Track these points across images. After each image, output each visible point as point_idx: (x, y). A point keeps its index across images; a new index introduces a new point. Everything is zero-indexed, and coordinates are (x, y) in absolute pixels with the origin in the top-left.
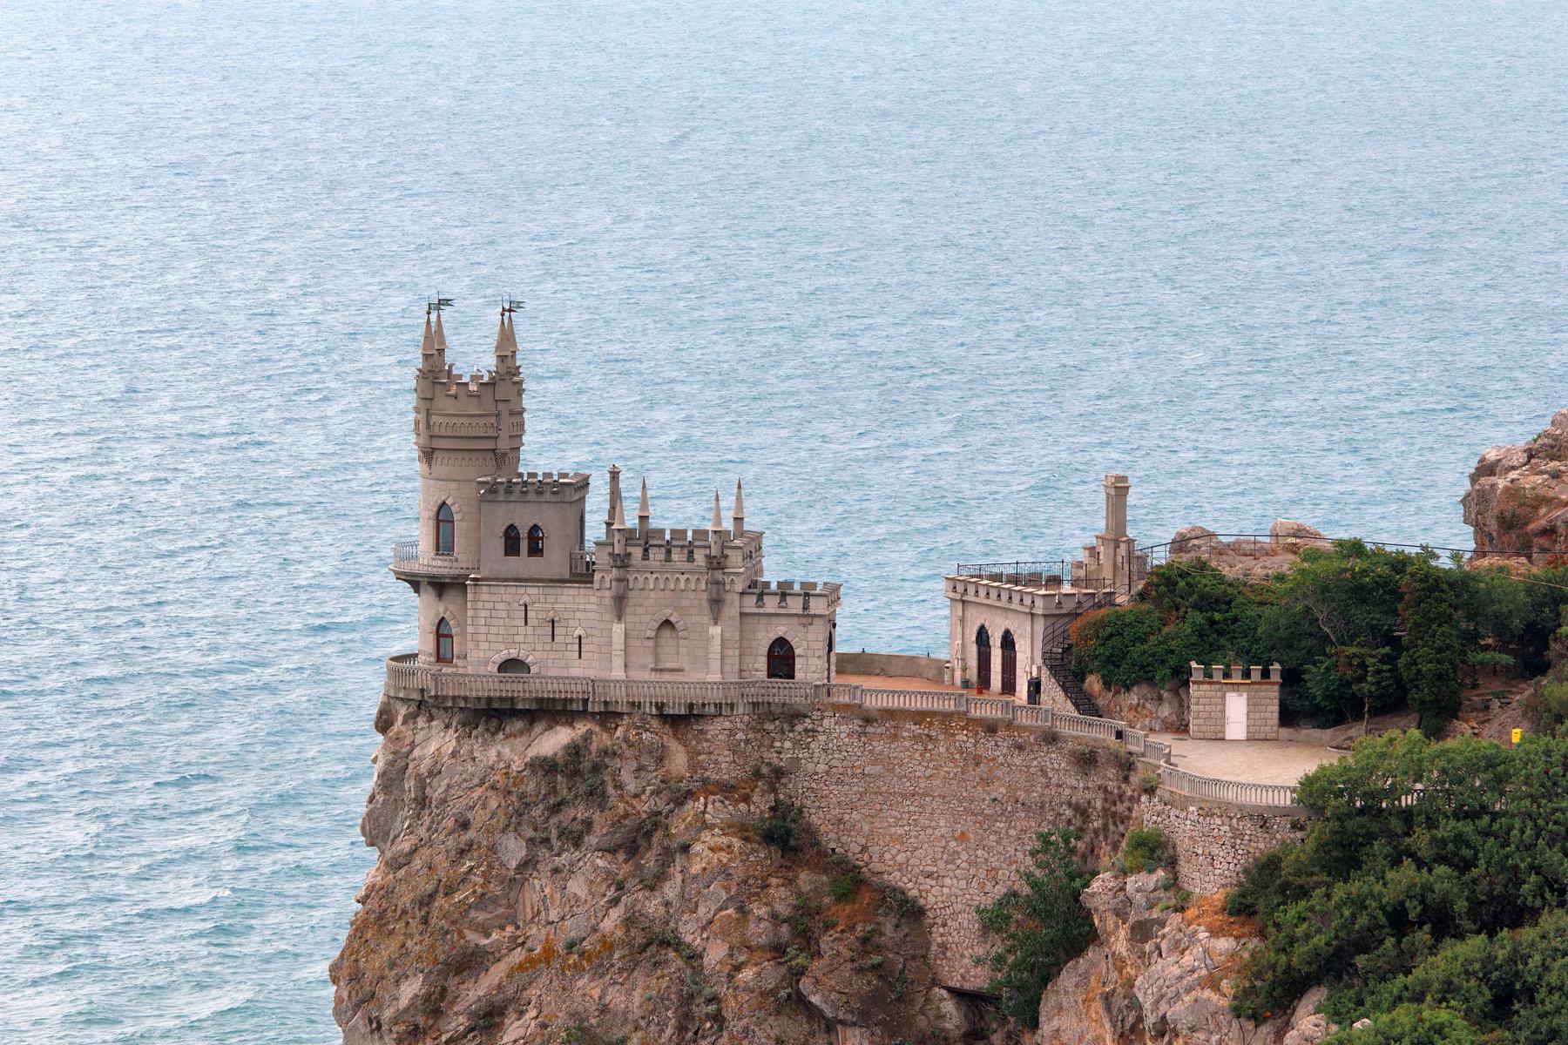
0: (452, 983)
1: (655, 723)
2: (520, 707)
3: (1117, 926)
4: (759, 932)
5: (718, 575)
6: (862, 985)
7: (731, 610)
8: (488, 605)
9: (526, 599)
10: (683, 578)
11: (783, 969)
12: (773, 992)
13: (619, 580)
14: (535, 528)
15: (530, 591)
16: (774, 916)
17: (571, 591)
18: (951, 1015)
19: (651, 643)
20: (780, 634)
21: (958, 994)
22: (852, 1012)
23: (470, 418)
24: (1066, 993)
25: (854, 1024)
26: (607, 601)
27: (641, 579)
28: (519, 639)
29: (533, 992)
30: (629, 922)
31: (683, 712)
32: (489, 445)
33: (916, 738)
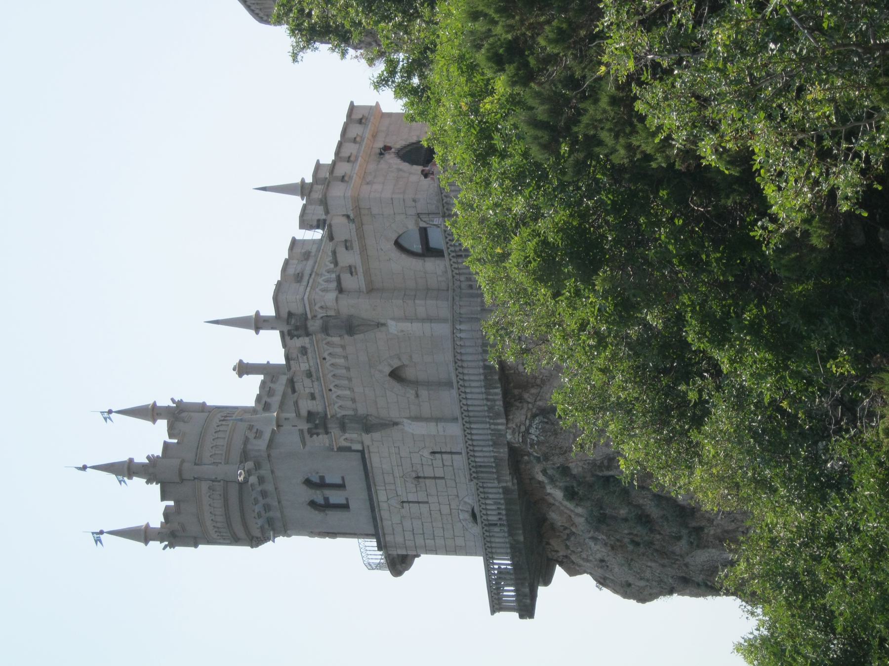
1: (520, 416)
2: (521, 538)
5: (314, 325)
7: (362, 307)
8: (409, 535)
9: (393, 502)
10: (330, 360)
13: (343, 427)
14: (308, 482)
15: (382, 496)
17: (375, 461)
19: (424, 393)
20: (390, 245)
23: (220, 484)
26: (376, 435)
27: (340, 403)
28: (445, 510)
31: (498, 391)
32: (233, 492)
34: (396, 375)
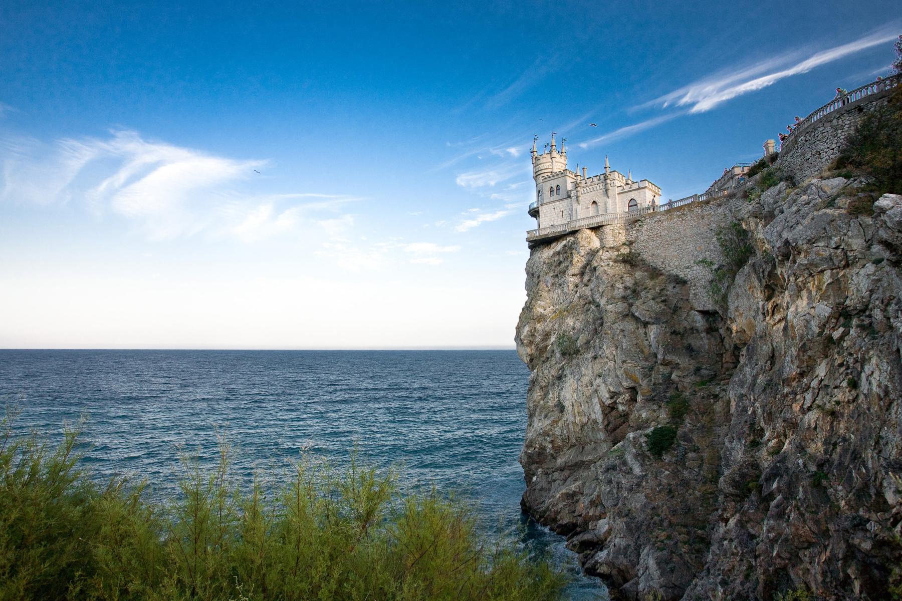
0: (538, 326)
3: (757, 225)
4: (619, 291)
5: (608, 181)
6: (658, 307)
11: (626, 305)
12: (620, 313)
16: (626, 288)
18: (700, 322)
21: (705, 313)
22: (651, 317)
24: (740, 286)
25: (653, 323)
29: (556, 326)
30: (580, 297)
33: (679, 217)
34: (594, 202)
